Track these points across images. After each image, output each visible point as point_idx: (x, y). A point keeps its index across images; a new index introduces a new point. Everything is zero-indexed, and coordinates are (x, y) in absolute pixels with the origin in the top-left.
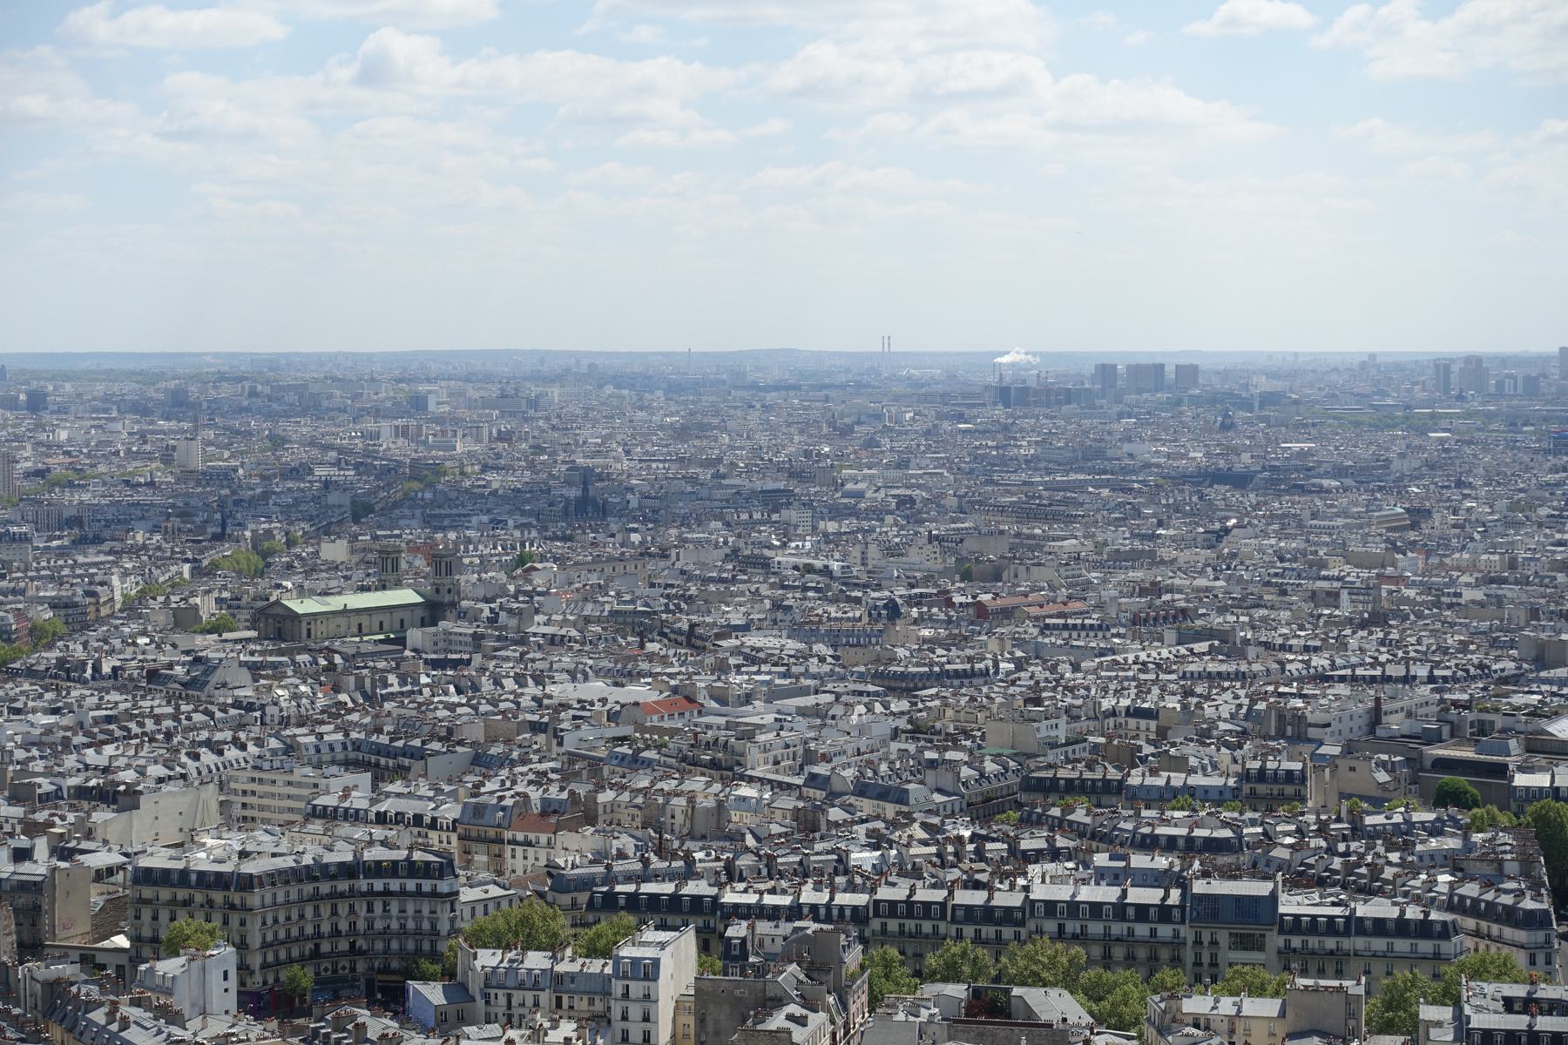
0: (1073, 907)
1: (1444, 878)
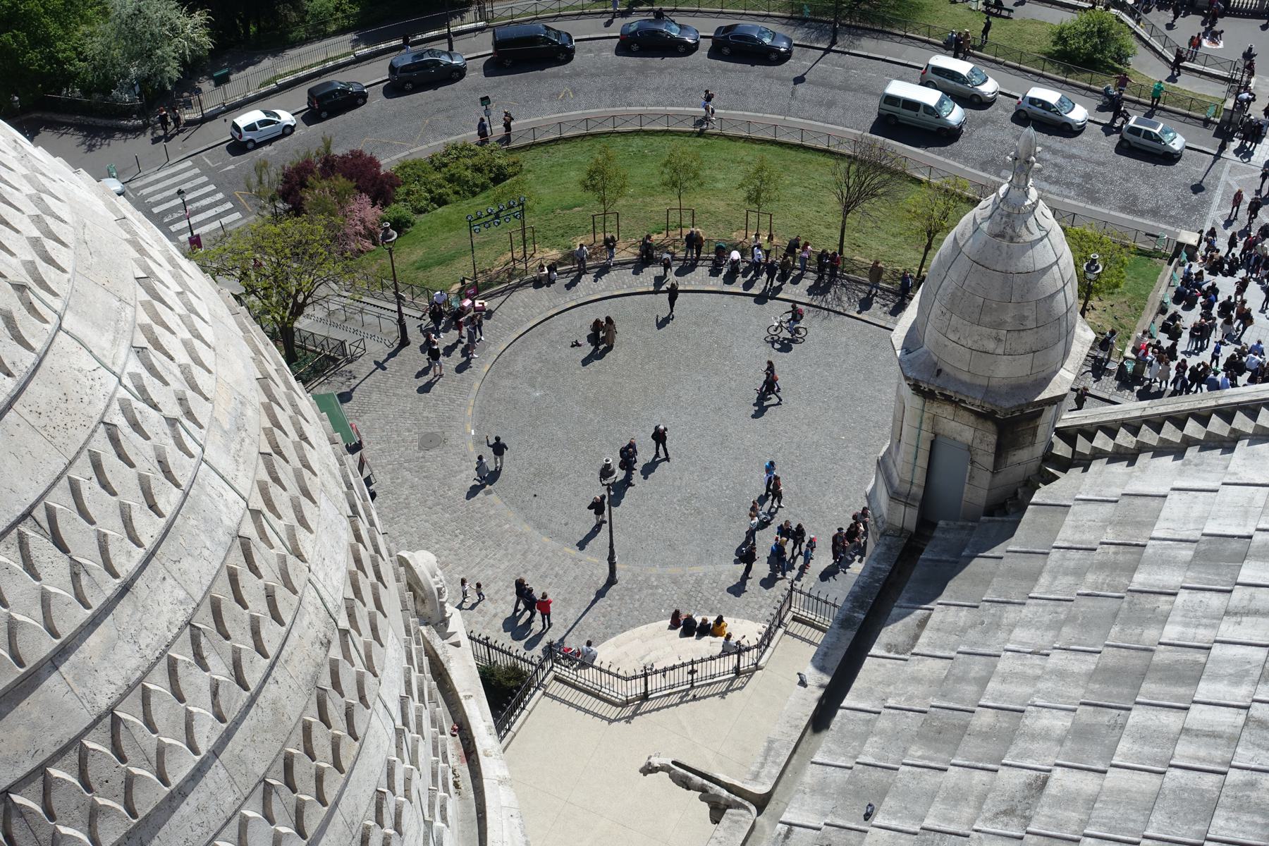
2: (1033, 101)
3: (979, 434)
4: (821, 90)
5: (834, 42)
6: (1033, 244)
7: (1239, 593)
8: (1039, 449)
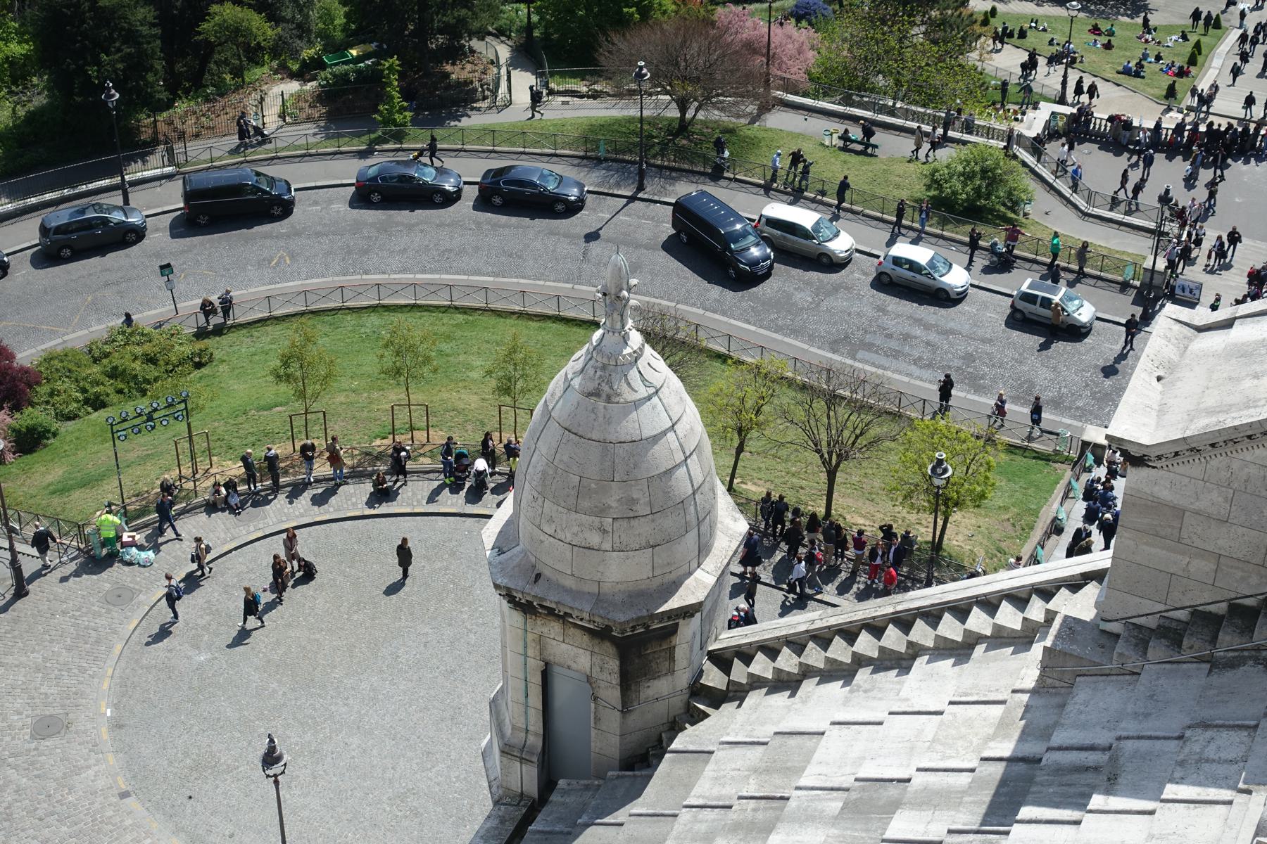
2: (897, 261)
3: (597, 659)
5: (641, 188)
6: (637, 404)
8: (682, 679)
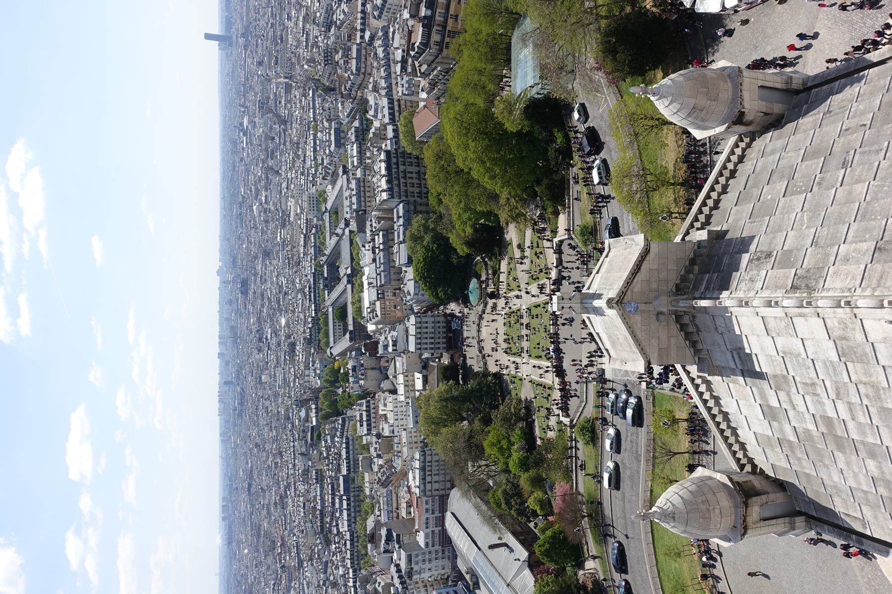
0: (349, 520)
1: (336, 439)
2: (611, 448)
4: (628, 527)
5: (610, 525)
6: (673, 505)
7: (784, 406)
8: (751, 477)
